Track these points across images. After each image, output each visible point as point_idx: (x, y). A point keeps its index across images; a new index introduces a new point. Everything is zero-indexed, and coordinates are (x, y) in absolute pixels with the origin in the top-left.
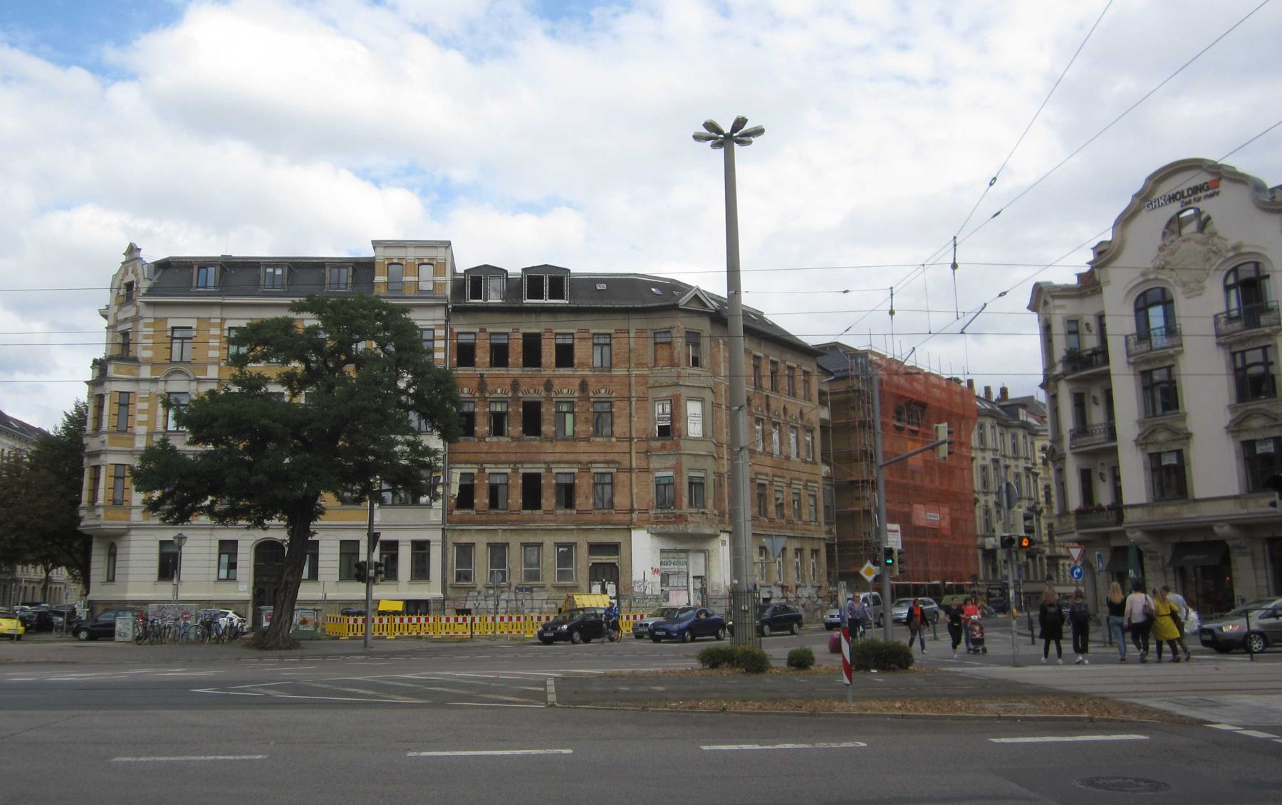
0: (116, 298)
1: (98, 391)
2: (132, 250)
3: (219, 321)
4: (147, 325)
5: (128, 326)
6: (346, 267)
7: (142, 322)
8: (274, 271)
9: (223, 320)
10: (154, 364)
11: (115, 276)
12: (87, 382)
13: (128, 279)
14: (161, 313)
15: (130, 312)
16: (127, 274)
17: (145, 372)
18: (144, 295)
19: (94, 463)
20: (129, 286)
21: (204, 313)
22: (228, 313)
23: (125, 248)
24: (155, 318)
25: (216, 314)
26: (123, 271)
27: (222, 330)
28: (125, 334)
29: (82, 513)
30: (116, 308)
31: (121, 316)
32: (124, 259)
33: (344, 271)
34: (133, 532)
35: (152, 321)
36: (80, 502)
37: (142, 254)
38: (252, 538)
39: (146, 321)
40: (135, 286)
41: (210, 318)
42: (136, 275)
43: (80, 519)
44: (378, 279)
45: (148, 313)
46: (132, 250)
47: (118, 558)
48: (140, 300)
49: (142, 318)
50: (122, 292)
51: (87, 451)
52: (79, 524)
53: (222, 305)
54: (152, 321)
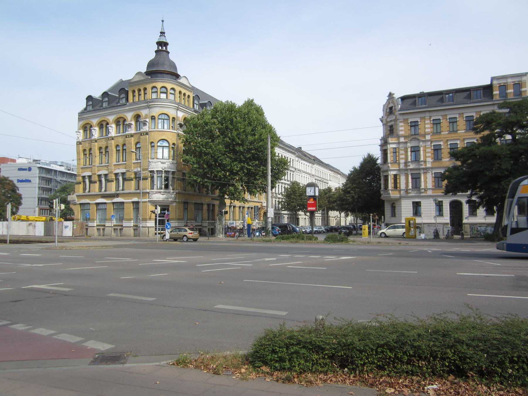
0: (386, 114)
1: (384, 148)
2: (391, 95)
3: (429, 117)
4: (401, 122)
5: (392, 123)
6: (480, 90)
7: (398, 121)
8: (449, 95)
9: (430, 117)
10: (405, 137)
11: (384, 106)
12: (379, 145)
13: (390, 106)
14: (406, 117)
15: (392, 117)
16: (390, 104)
17: (402, 140)
18: (399, 111)
19: (385, 174)
20: (391, 108)
21: (422, 115)
22: (431, 114)
23: (388, 94)
24: (404, 119)
25: (427, 114)
26: (387, 103)
27: (430, 121)
28: (391, 126)
29: (382, 192)
30: (386, 117)
31: (389, 120)
32: (387, 98)
33: (479, 92)
34: (402, 199)
35: (402, 120)
36: (381, 189)
37: (394, 96)
38: (448, 199)
39: (400, 120)
40: (394, 108)
41: (425, 117)
42: (394, 104)
43: (380, 195)
44: (494, 93)
45: (401, 118)
46: (391, 95)
47: (396, 208)
48: (397, 113)
49: (398, 119)
50: (388, 111)
51: (381, 170)
52: (381, 196)
53: (430, 111)
54: (402, 120)
